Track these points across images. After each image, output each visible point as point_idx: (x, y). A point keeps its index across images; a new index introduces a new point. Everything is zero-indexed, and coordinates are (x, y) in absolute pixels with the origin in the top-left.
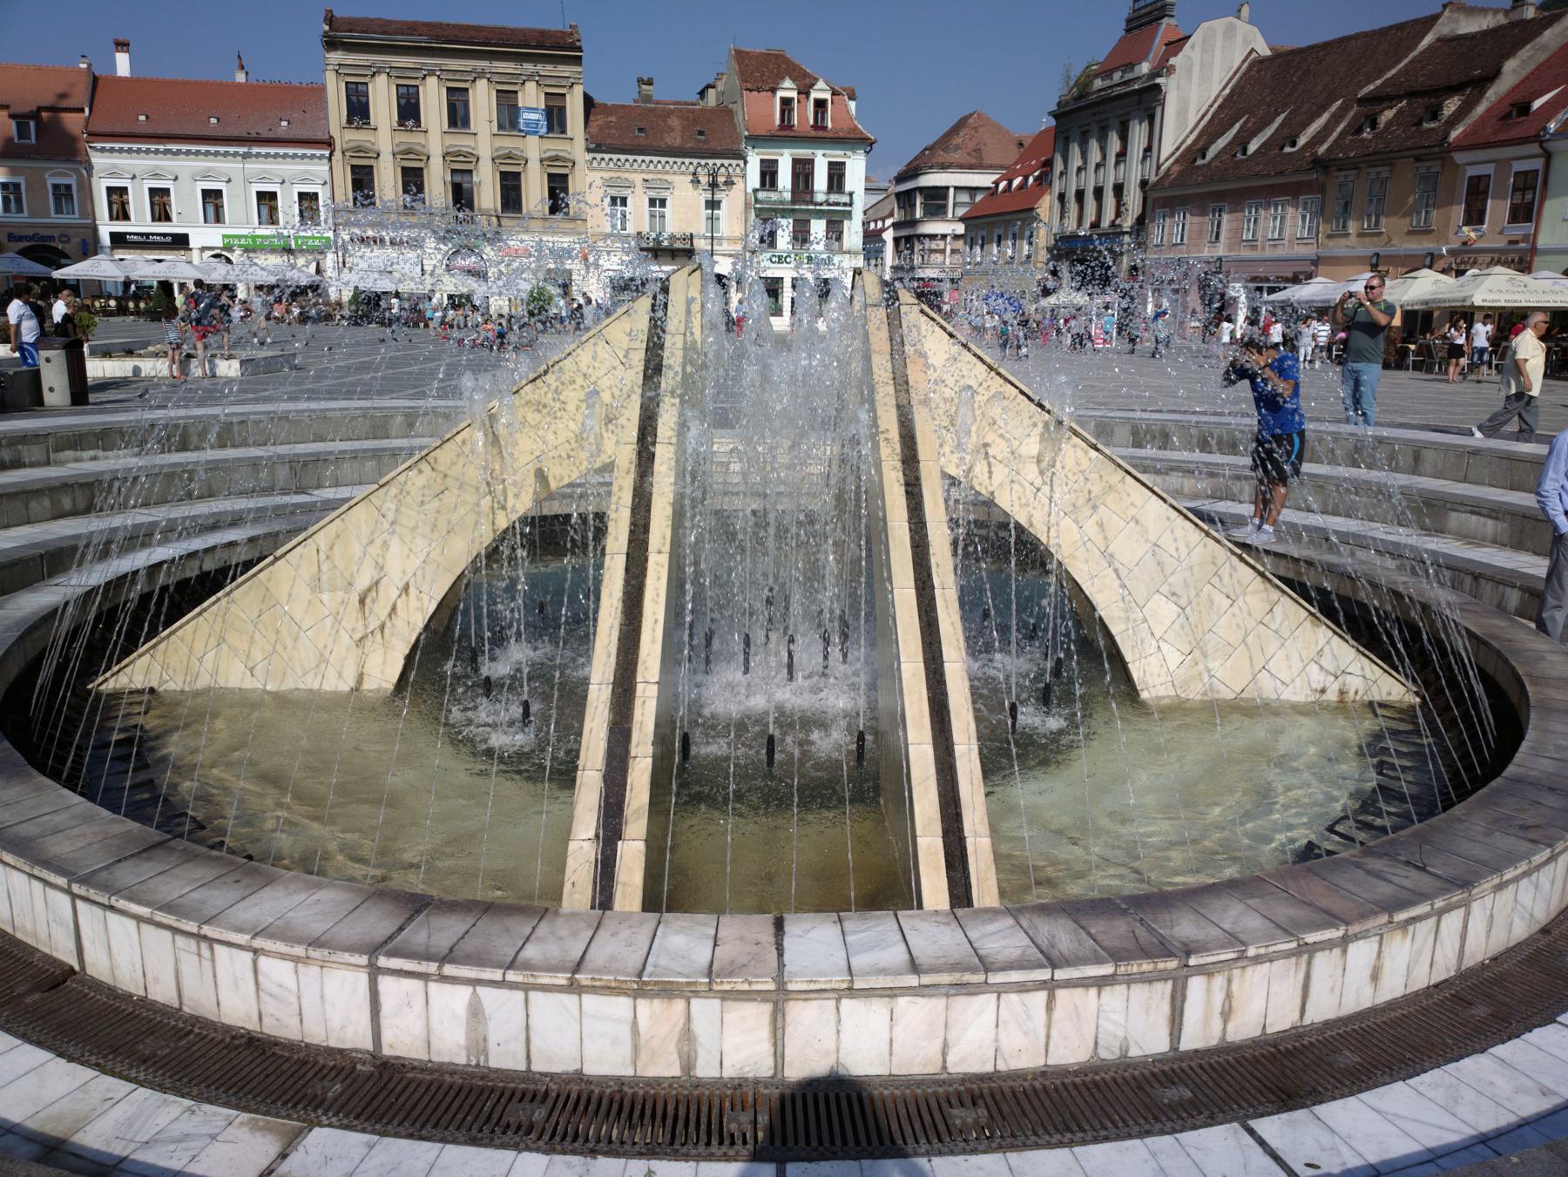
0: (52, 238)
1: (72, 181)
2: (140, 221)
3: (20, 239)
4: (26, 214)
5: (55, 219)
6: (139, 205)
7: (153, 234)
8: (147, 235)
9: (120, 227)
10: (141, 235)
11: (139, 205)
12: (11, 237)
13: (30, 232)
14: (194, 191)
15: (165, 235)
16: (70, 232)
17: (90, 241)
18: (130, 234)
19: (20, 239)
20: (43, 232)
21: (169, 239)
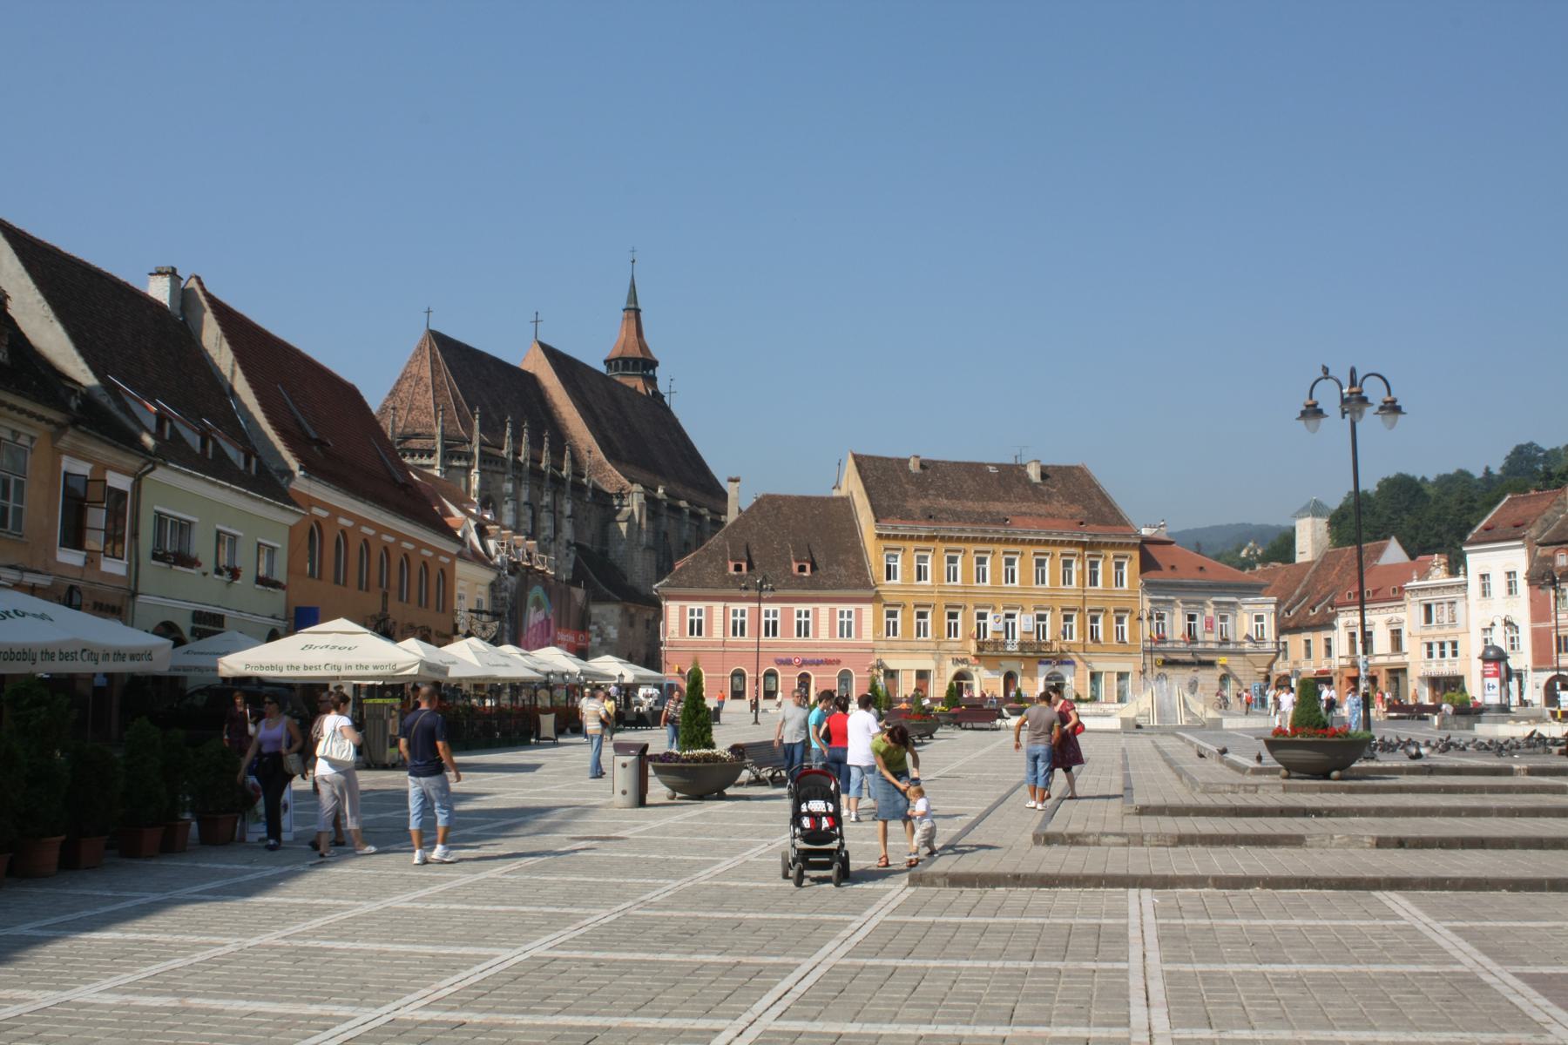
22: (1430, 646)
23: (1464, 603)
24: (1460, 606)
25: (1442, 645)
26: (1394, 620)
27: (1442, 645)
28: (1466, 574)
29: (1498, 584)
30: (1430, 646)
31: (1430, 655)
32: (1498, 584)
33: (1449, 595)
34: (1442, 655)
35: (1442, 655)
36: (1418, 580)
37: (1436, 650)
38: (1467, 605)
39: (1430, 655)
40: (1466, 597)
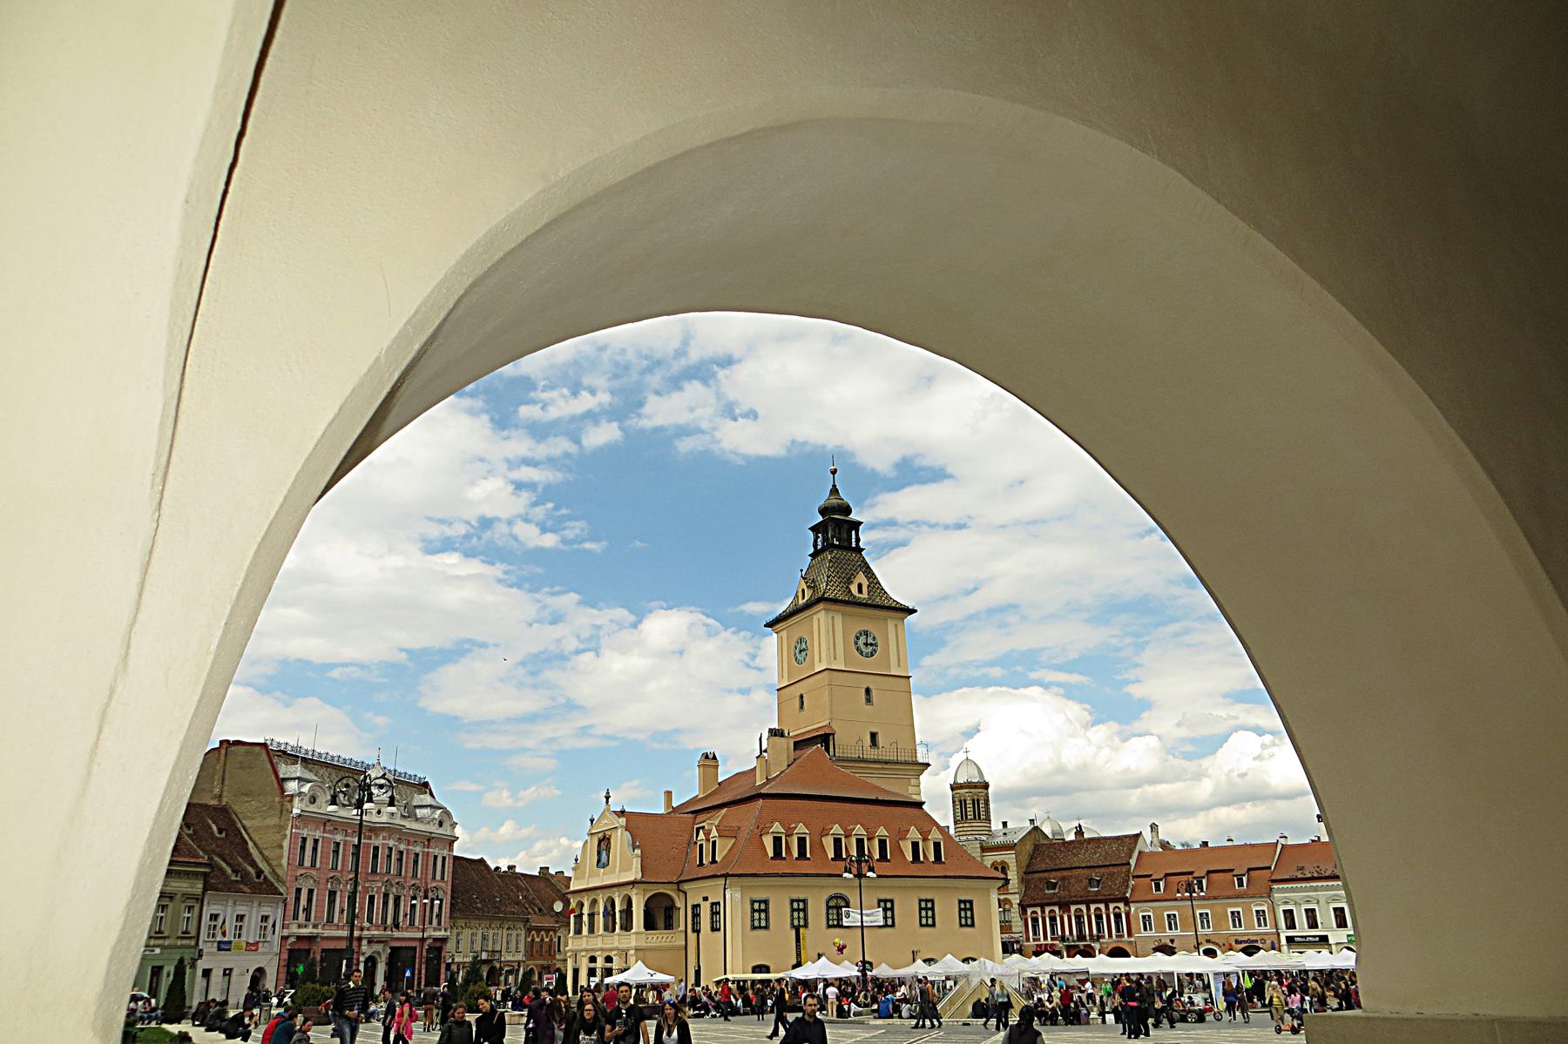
0: (1257, 941)
1: (1265, 908)
2: (1302, 929)
3: (1241, 942)
4: (1268, 927)
5: (1258, 930)
6: (1301, 919)
7: (1309, 936)
8: (1305, 937)
9: (1291, 933)
10: (1302, 937)
11: (1301, 919)
12: (1237, 942)
13: (1246, 938)
14: (1328, 909)
15: (1314, 937)
16: (1266, 937)
17: (1276, 942)
18: (1297, 937)
19: (1241, 942)
20: (1252, 938)
21: (1317, 939)
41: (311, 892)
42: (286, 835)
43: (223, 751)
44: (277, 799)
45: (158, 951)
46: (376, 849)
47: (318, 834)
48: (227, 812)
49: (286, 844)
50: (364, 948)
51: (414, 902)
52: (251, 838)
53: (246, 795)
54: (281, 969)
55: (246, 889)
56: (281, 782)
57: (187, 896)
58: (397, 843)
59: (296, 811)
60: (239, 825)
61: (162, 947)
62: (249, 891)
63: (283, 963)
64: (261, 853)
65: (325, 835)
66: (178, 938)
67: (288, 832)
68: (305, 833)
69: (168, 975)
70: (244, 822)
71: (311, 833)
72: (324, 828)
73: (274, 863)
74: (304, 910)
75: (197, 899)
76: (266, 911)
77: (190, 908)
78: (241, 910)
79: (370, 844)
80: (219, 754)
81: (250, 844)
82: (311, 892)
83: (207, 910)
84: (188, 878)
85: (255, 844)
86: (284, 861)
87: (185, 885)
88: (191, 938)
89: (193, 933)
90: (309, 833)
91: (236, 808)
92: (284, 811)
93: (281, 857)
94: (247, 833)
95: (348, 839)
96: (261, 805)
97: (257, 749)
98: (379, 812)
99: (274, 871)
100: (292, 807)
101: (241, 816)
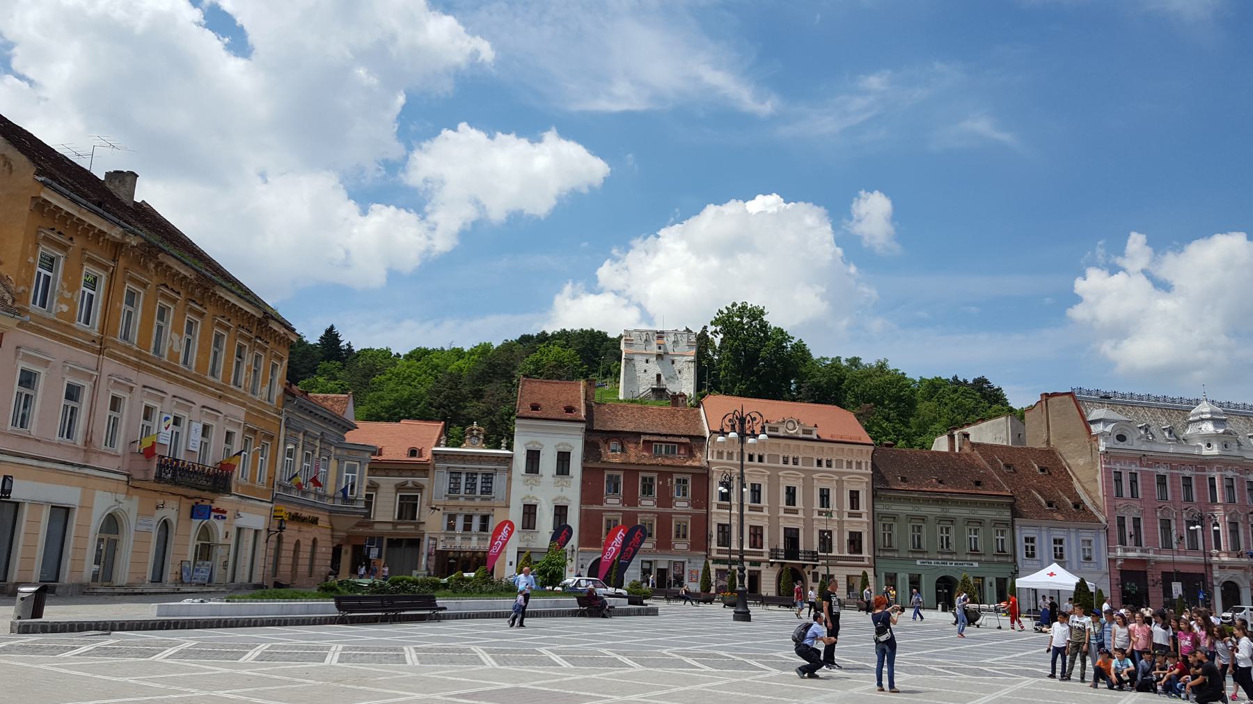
22: (452, 517)
23: (506, 476)
24: (498, 482)
25: (468, 518)
26: (410, 485)
27: (468, 518)
28: (509, 447)
29: (548, 463)
30: (452, 517)
31: (451, 527)
32: (548, 463)
33: (489, 467)
34: (467, 527)
35: (467, 527)
36: (447, 446)
37: (460, 523)
38: (510, 479)
39: (451, 527)
40: (510, 470)
41: (1136, 521)
42: (1097, 471)
43: (1044, 403)
44: (1087, 440)
45: (976, 565)
46: (1212, 479)
47: (1134, 469)
48: (1054, 453)
49: (1099, 477)
50: (1216, 574)
51: (1216, 528)
52: (1074, 474)
53: (1066, 438)
54: (1114, 587)
55: (1060, 517)
56: (1088, 424)
57: (996, 523)
58: (1238, 474)
59: (1102, 449)
60: (1064, 463)
61: (979, 562)
62: (1063, 519)
63: (1114, 582)
64: (1083, 487)
65: (1143, 469)
66: (967, 554)
67: (1099, 467)
68: (1118, 467)
69: (991, 585)
70: (1068, 461)
71: (1126, 468)
72: (1141, 462)
73: (1093, 495)
74: (1131, 536)
75: (1007, 524)
76: (1087, 535)
77: (1003, 533)
78: (1058, 534)
79: (1205, 476)
80: (1042, 406)
81: (1074, 479)
82: (1136, 521)
83: (1021, 534)
84: (967, 506)
85: (1078, 479)
86: (1100, 494)
87: (994, 513)
88: (1007, 556)
89: (1008, 549)
90: (1123, 467)
91: (1061, 450)
92: (1093, 450)
93: (1097, 490)
94: (1071, 470)
95: (1174, 471)
96: (1076, 445)
97: (1067, 397)
98: (1209, 445)
99: (1094, 502)
100: (1099, 445)
101: (1065, 456)
